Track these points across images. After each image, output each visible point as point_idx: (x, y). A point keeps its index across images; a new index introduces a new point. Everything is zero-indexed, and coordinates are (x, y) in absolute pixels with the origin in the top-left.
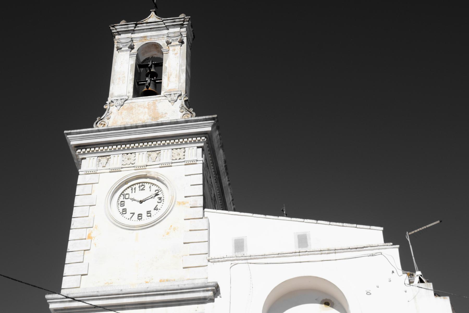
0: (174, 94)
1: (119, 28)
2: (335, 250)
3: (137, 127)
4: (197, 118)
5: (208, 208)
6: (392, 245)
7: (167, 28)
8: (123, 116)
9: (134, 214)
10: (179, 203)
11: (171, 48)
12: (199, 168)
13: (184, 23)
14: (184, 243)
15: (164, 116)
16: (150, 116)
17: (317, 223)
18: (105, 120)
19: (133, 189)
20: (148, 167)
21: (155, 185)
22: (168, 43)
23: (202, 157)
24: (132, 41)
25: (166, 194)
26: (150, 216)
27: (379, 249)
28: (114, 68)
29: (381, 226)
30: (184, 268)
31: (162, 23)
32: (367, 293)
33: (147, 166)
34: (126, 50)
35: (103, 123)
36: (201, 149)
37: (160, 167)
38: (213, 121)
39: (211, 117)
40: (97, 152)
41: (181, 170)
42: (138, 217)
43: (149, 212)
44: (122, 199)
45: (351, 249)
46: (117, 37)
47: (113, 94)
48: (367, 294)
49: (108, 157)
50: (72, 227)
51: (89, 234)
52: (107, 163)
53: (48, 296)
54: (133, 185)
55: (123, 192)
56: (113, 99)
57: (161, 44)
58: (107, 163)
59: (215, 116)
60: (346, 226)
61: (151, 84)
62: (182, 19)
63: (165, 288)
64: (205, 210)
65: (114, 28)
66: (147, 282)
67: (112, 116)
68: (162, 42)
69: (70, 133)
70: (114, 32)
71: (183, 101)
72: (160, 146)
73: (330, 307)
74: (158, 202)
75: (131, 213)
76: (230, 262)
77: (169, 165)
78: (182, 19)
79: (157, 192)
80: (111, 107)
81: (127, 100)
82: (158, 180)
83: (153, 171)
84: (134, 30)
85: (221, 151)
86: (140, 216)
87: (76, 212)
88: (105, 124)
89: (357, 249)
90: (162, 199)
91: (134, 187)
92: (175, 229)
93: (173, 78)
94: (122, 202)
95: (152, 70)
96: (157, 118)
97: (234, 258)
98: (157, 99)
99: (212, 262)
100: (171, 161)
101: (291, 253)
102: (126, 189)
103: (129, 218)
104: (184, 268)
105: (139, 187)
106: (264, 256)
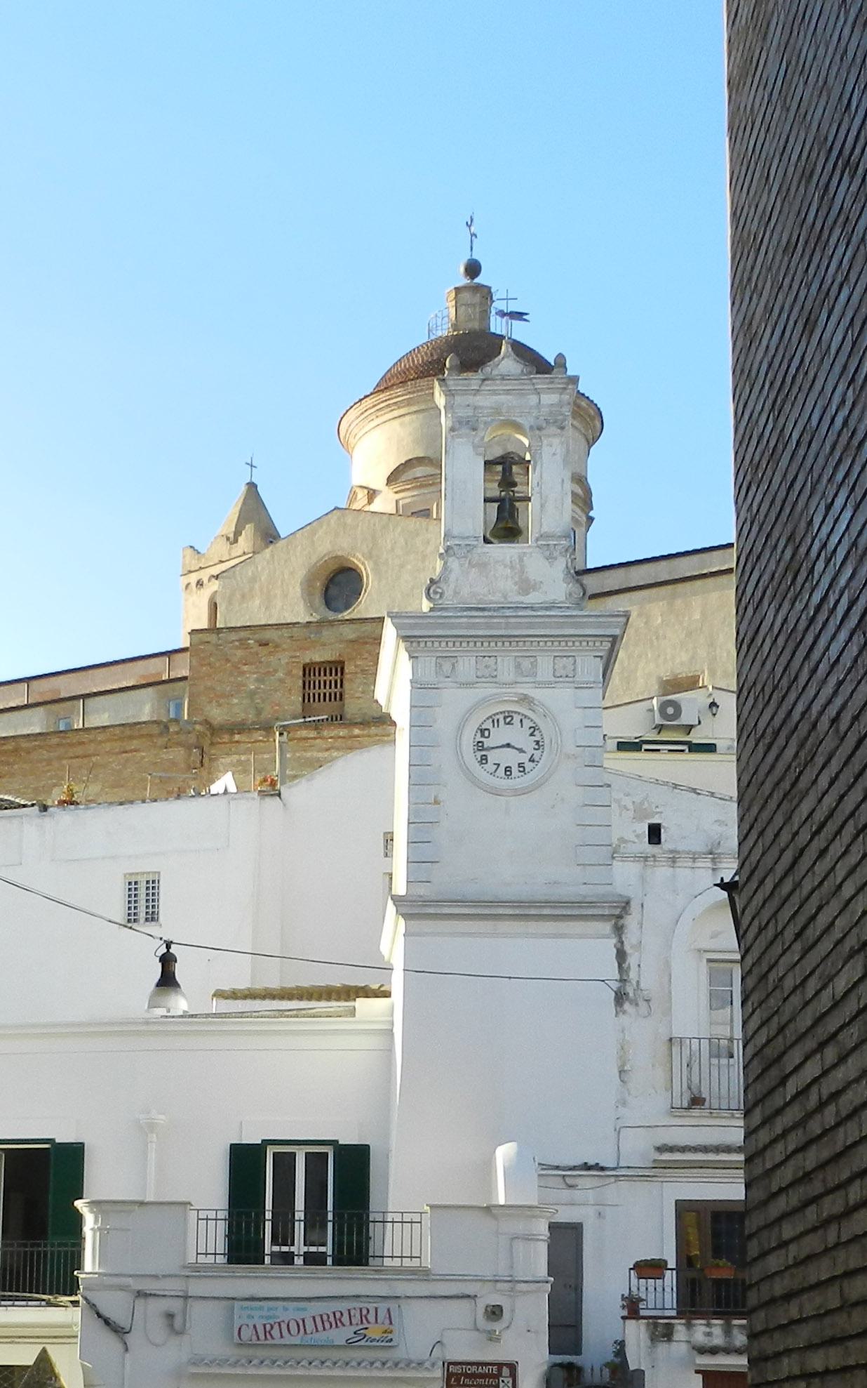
0: (555, 545)
9: (499, 765)
16: (516, 583)
19: (496, 721)
21: (529, 718)
35: (440, 591)
42: (506, 771)
43: (520, 765)
44: (479, 738)
49: (454, 660)
74: (535, 749)
75: (495, 764)
79: (532, 730)
84: (478, 390)
90: (541, 744)
94: (479, 742)
100: (553, 679)
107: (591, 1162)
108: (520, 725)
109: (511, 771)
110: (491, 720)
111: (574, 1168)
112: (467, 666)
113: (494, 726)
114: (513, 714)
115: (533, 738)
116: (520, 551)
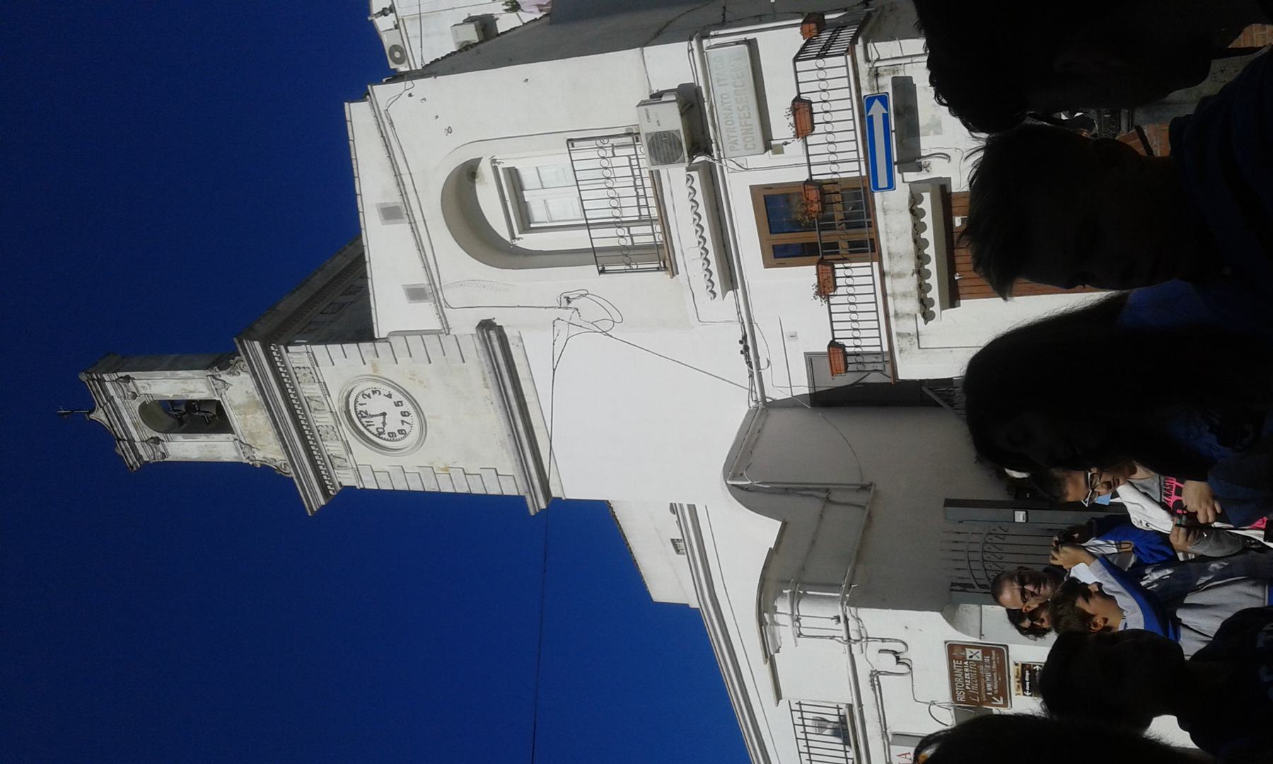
0: (214, 385)
1: (131, 460)
2: (396, 175)
3: (280, 434)
4: (242, 353)
5: (373, 334)
6: (370, 96)
7: (110, 399)
8: (266, 444)
9: (403, 422)
10: (375, 371)
11: (142, 391)
12: (319, 350)
13: (96, 378)
14: (430, 362)
15: (251, 395)
16: (257, 412)
17: (361, 195)
18: (278, 464)
20: (333, 410)
21: (356, 399)
22: (135, 396)
23: (300, 344)
24: (146, 441)
25: (367, 386)
26: (401, 402)
27: (380, 114)
28: (196, 459)
29: (343, 106)
30: (464, 362)
31: (105, 408)
32: (448, 132)
33: (331, 412)
34: (164, 447)
35: (283, 467)
36: (289, 347)
37: (329, 396)
38: (244, 341)
39: (239, 346)
40: (328, 471)
41: (326, 371)
42: (405, 416)
43: (397, 404)
44: (386, 436)
45: (389, 153)
46: (146, 459)
47: (235, 457)
48: (450, 133)
49: (332, 457)
50: (437, 490)
51: (442, 470)
52: (340, 458)
53: (532, 512)
54: (363, 425)
55: (375, 435)
56: (244, 458)
57: (139, 404)
58: (340, 458)
59: (236, 340)
60: (355, 154)
61: (206, 410)
62: (91, 382)
63: (496, 387)
64: (376, 336)
65: (134, 466)
66: (492, 403)
67: (270, 456)
68: (136, 404)
69: (310, 508)
70: (140, 463)
71: (221, 373)
72: (299, 399)
73: (477, 169)
74: (380, 394)
76: (445, 309)
77: (324, 386)
78: (91, 382)
79: (365, 396)
80: (257, 458)
81: (240, 441)
82: (348, 396)
83: (337, 404)
84: (129, 441)
85: (281, 307)
86: (404, 414)
87: (416, 486)
88: (285, 464)
89: (388, 144)
91: (366, 424)
92: (413, 375)
93: (191, 387)
94: (390, 436)
95: (184, 410)
96: (257, 403)
97: (438, 304)
98: (227, 404)
99: (449, 331)
101: (415, 235)
102: (370, 432)
103: (409, 426)
104: (464, 362)
105: (365, 417)
106: (427, 267)
107: (741, 347)
108: (364, 406)
109: (405, 412)
110: (368, 427)
111: (749, 364)
112: (332, 447)
113: (373, 425)
114: (358, 410)
115: (372, 395)
116: (229, 408)
